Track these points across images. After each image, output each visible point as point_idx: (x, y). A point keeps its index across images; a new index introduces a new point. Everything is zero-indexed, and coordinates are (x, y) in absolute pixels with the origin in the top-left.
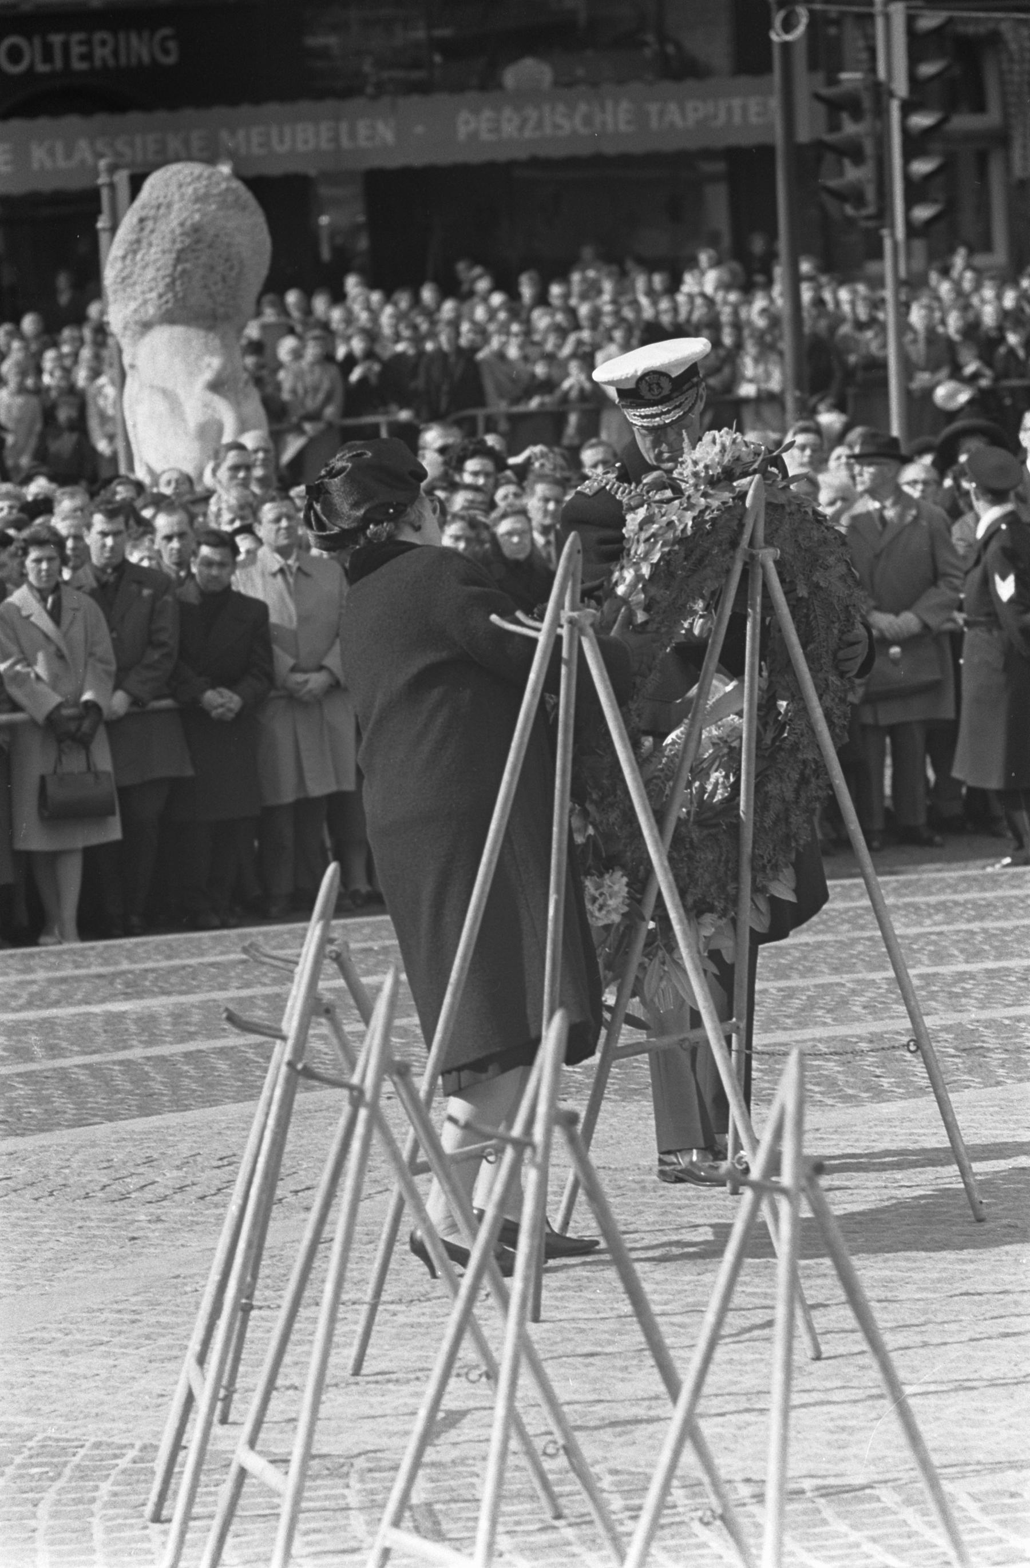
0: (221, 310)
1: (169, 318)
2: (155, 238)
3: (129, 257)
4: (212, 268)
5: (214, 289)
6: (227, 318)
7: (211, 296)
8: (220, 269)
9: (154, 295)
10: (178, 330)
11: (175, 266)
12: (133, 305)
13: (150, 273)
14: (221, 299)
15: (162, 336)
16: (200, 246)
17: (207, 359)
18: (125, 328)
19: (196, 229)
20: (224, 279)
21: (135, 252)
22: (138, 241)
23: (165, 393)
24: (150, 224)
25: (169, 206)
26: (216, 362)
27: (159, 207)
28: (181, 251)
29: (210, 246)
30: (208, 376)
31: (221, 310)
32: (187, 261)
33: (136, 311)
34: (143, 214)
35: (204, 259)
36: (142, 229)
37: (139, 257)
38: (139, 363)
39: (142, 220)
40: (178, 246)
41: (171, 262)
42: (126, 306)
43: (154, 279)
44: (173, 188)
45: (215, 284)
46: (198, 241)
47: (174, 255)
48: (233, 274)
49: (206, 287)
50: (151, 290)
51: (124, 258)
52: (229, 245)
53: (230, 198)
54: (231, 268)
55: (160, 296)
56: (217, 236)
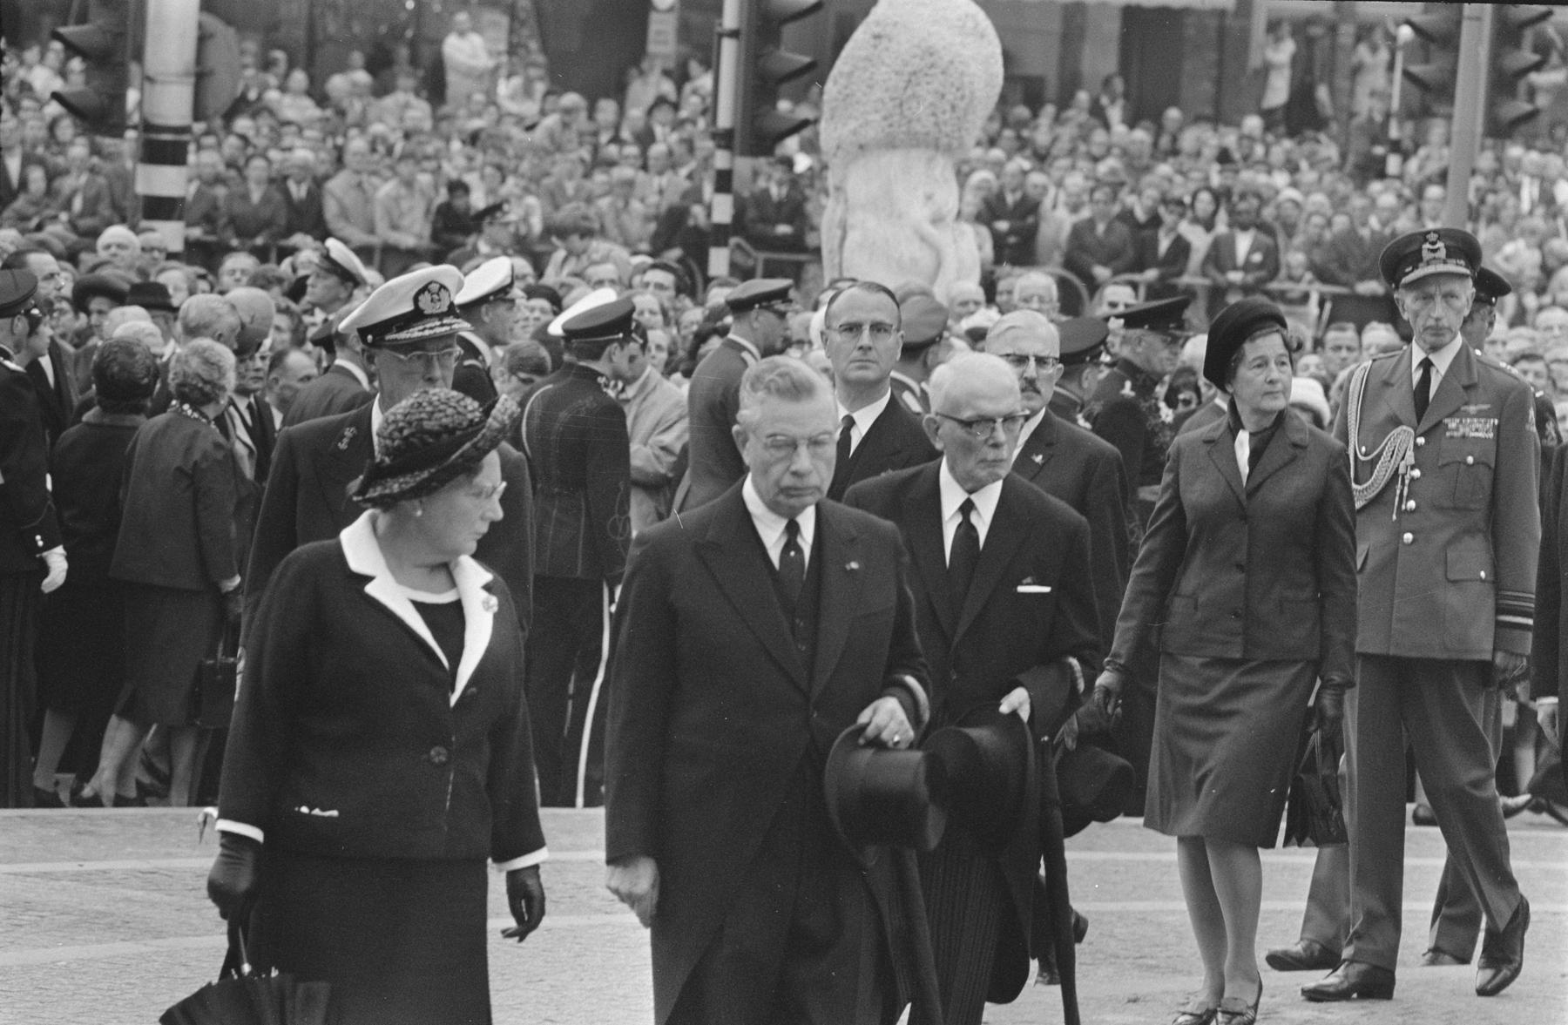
0: (944, 141)
3: (857, 74)
4: (943, 96)
5: (942, 118)
8: (950, 97)
9: (877, 117)
11: (906, 88)
12: (853, 125)
14: (947, 129)
16: (933, 71)
18: (838, 147)
19: (931, 53)
20: (953, 108)
22: (868, 59)
24: (884, 43)
27: (895, 24)
28: (914, 73)
29: (943, 73)
31: (944, 141)
32: (918, 84)
33: (854, 132)
34: (877, 30)
35: (935, 85)
36: (875, 47)
37: (868, 74)
40: (909, 69)
41: (902, 85)
42: (845, 125)
43: (882, 101)
45: (944, 112)
46: (932, 66)
47: (906, 78)
48: (962, 105)
49: (934, 114)
50: (877, 111)
51: (850, 74)
52: (962, 74)
53: (970, 24)
54: (963, 97)
55: (885, 118)
56: (952, 62)
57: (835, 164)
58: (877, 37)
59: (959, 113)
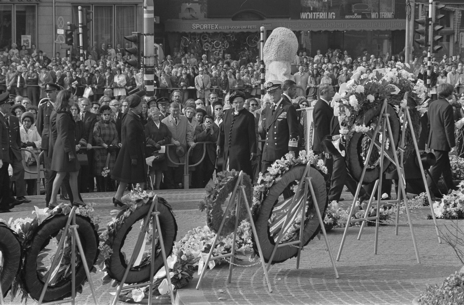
1: (277, 60)
2: (274, 43)
6: (288, 60)
7: (285, 55)
10: (278, 62)
12: (269, 57)
13: (273, 50)
15: (274, 64)
17: (284, 69)
19: (283, 41)
21: (270, 45)
23: (274, 75)
25: (277, 36)
26: (285, 70)
30: (284, 72)
38: (269, 69)
39: (272, 39)
44: (279, 32)
57: (266, 64)
58: (272, 39)
59: (289, 53)
